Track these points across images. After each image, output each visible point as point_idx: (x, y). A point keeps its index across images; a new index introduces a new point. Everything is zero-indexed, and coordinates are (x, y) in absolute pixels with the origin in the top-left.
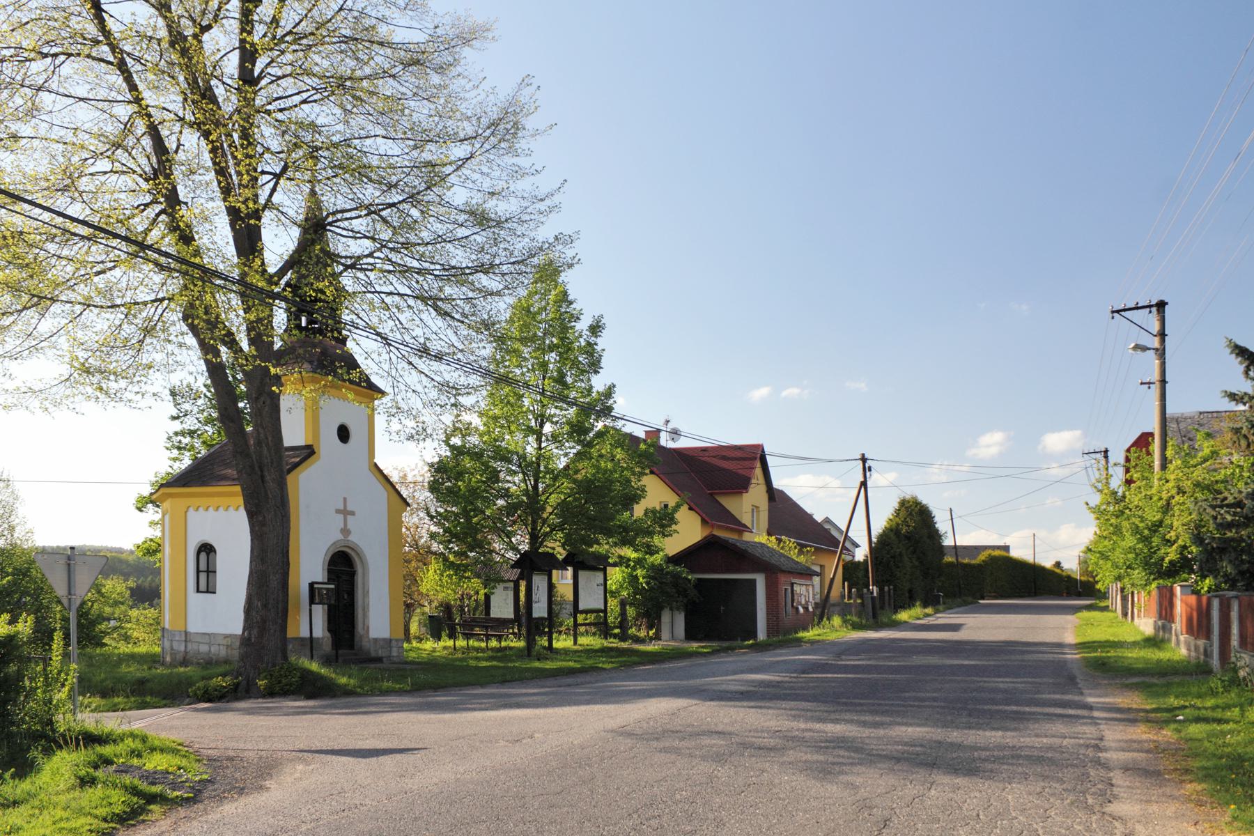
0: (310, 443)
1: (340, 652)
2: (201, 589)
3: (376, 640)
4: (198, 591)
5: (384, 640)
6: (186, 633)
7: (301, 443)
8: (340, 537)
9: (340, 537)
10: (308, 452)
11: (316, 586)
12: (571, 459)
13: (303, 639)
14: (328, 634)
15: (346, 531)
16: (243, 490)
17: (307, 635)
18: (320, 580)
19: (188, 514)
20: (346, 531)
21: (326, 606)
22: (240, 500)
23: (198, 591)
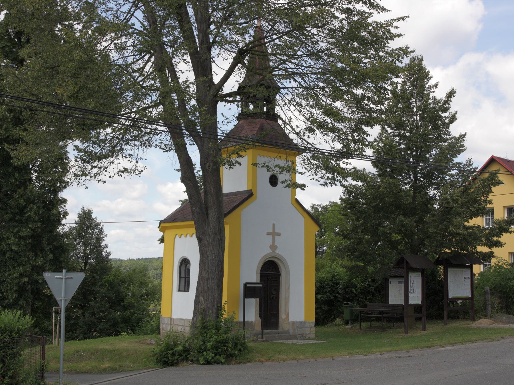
0: (251, 189)
1: (265, 331)
2: (181, 290)
3: (294, 323)
4: (179, 290)
5: (301, 322)
6: (171, 318)
7: (245, 189)
8: (270, 251)
9: (270, 251)
10: (249, 195)
11: (248, 285)
12: (159, 77)
13: (240, 323)
14: (259, 319)
15: (273, 247)
16: (195, 223)
17: (242, 320)
18: (255, 281)
19: (176, 239)
20: (273, 247)
21: (258, 300)
22: (193, 230)
23: (179, 290)
